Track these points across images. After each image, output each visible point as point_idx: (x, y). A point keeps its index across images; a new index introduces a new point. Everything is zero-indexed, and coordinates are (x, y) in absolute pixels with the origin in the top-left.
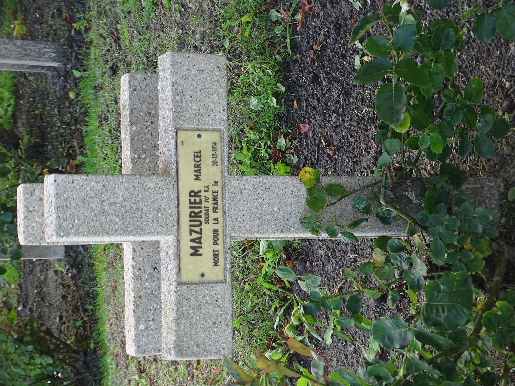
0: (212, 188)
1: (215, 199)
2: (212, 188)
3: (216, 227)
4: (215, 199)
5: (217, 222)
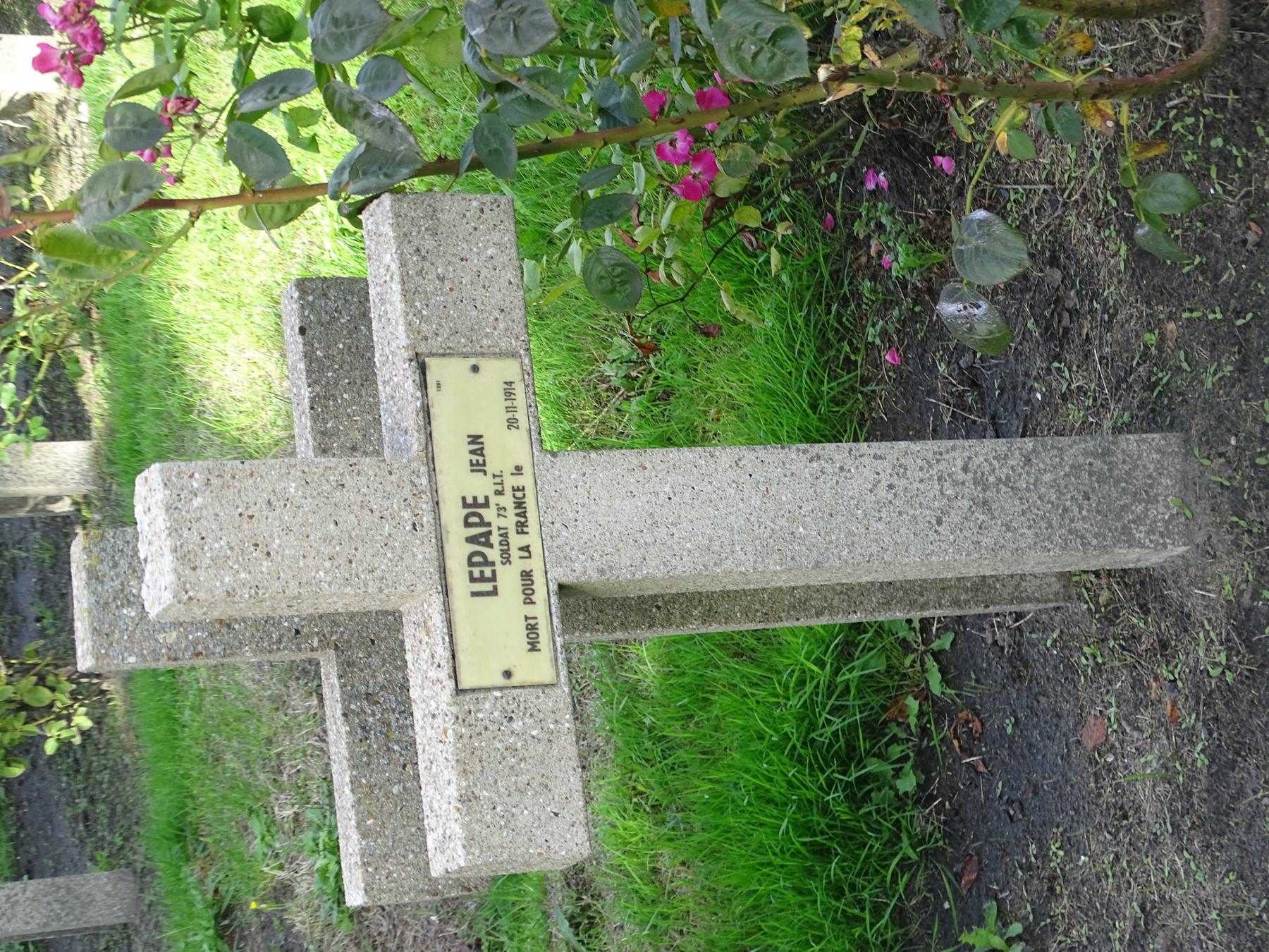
0: (510, 482)
1: (519, 504)
2: (510, 482)
3: (527, 565)
4: (519, 504)
5: (527, 554)
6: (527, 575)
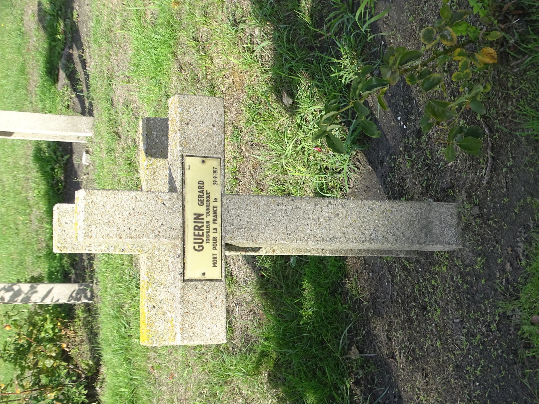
1: (215, 212)
3: (215, 235)
4: (215, 212)
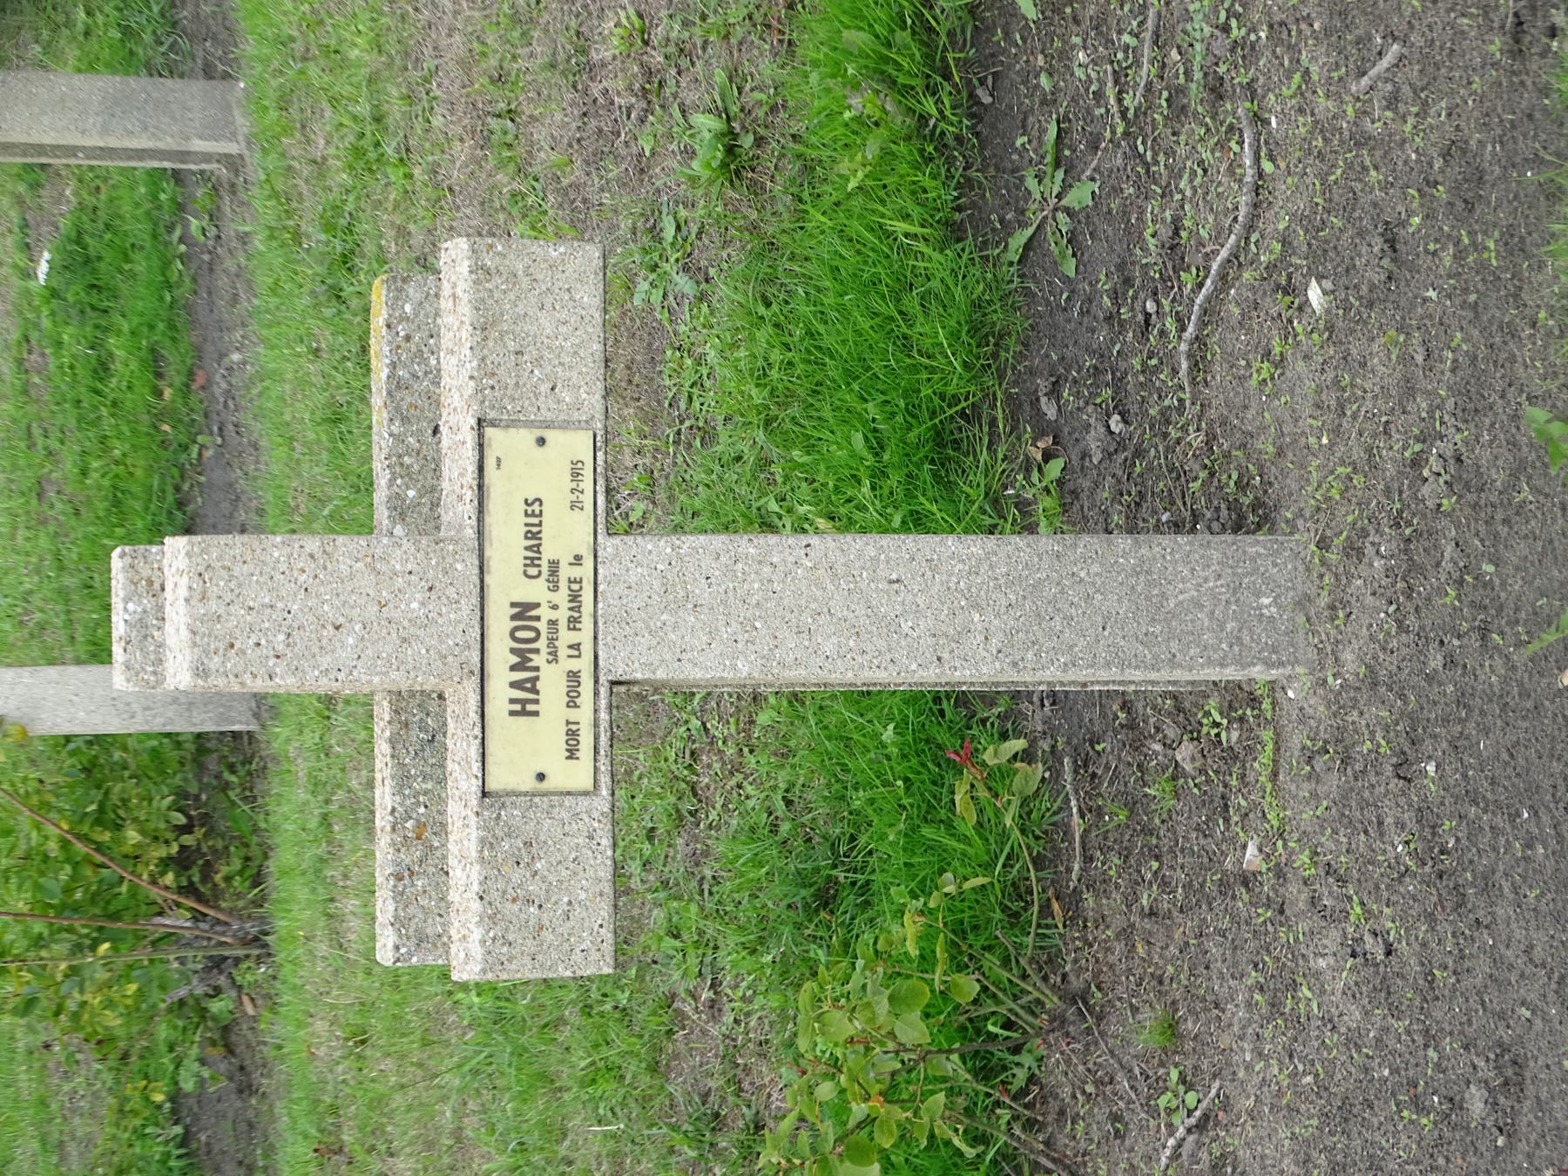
1: (575, 597)
2: (566, 572)
3: (574, 665)
4: (575, 597)
6: (574, 676)
